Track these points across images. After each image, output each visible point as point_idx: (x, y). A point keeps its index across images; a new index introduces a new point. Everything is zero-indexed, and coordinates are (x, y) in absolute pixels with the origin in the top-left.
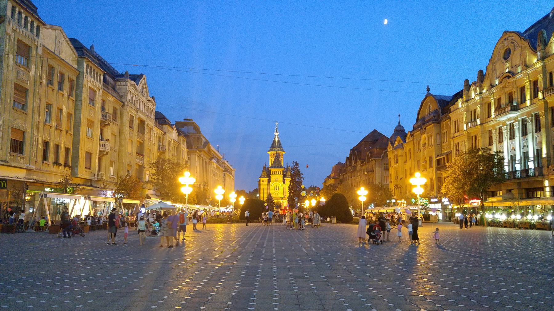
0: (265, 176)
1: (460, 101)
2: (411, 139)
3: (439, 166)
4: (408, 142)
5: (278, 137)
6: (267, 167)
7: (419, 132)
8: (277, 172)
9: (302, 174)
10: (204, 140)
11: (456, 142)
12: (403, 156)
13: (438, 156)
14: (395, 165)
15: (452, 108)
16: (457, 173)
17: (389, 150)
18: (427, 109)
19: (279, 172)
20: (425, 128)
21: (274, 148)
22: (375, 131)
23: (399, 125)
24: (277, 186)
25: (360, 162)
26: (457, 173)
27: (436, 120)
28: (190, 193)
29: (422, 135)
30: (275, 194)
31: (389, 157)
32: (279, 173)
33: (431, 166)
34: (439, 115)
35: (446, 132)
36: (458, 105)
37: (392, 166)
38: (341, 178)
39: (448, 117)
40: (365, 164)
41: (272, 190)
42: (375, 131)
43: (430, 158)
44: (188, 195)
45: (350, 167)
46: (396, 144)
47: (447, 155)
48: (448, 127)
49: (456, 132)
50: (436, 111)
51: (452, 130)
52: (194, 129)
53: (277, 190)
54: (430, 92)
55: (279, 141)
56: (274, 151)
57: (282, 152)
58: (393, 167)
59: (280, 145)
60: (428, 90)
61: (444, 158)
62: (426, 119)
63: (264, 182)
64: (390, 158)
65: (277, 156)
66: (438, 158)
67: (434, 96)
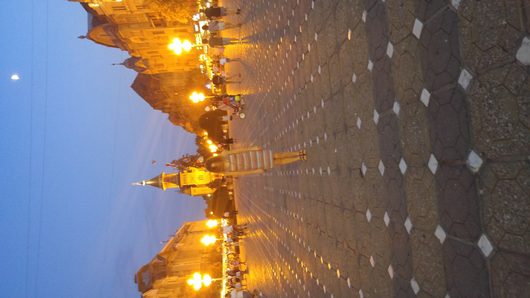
0: (189, 190)
1: (91, 5)
2: (137, 52)
3: (162, 25)
4: (140, 54)
5: (148, 181)
6: (180, 190)
7: (129, 45)
8: (184, 179)
9: (183, 156)
10: (156, 260)
11: (135, 9)
12: (155, 60)
13: (152, 26)
14: (165, 66)
15: (100, 13)
16: (166, 8)
17: (150, 73)
18: (104, 38)
20: (124, 39)
21: (160, 184)
22: (133, 86)
23: (124, 64)
24: (198, 178)
25: (166, 100)
26: (166, 8)
27: (114, 28)
28: (210, 277)
29: (131, 42)
30: (206, 178)
31: (158, 73)
32: (185, 177)
33: (163, 32)
34: (109, 26)
35: (126, 18)
36: (96, 7)
37: (167, 69)
38: (184, 117)
39: (110, 17)
40: (167, 94)
42: (133, 86)
43: (154, 33)
44: (212, 278)
45: (172, 109)
46: (143, 66)
47: (150, 17)
48: (120, 17)
49: (126, 9)
50: (105, 29)
51: (123, 13)
52: (145, 272)
53: (202, 178)
54: (85, 35)
55: (151, 180)
56: (162, 184)
57: (163, 176)
58: (167, 68)
59: (156, 179)
60: (82, 37)
61: (153, 20)
62: (114, 38)
64: (159, 71)
65: (168, 180)
66: (154, 26)
67: (90, 31)
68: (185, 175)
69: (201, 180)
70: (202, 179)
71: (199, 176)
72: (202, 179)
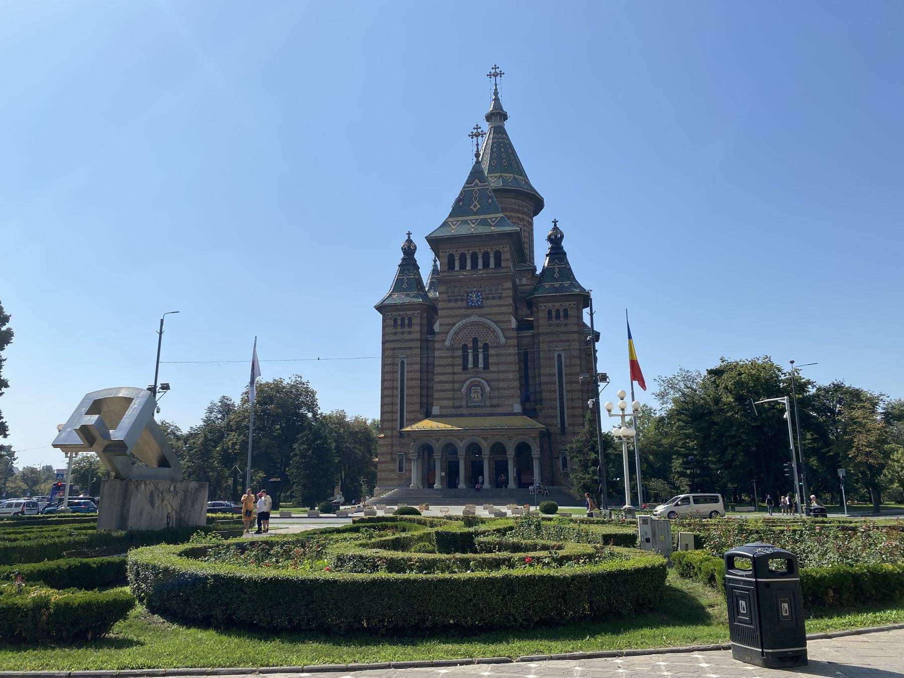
19: (486, 256)
24: (475, 340)
30: (469, 390)
32: (486, 265)
41: (449, 361)
63: (406, 329)
68: (498, 264)
69: (459, 361)
70: (465, 368)
71: (486, 347)
72: (465, 368)
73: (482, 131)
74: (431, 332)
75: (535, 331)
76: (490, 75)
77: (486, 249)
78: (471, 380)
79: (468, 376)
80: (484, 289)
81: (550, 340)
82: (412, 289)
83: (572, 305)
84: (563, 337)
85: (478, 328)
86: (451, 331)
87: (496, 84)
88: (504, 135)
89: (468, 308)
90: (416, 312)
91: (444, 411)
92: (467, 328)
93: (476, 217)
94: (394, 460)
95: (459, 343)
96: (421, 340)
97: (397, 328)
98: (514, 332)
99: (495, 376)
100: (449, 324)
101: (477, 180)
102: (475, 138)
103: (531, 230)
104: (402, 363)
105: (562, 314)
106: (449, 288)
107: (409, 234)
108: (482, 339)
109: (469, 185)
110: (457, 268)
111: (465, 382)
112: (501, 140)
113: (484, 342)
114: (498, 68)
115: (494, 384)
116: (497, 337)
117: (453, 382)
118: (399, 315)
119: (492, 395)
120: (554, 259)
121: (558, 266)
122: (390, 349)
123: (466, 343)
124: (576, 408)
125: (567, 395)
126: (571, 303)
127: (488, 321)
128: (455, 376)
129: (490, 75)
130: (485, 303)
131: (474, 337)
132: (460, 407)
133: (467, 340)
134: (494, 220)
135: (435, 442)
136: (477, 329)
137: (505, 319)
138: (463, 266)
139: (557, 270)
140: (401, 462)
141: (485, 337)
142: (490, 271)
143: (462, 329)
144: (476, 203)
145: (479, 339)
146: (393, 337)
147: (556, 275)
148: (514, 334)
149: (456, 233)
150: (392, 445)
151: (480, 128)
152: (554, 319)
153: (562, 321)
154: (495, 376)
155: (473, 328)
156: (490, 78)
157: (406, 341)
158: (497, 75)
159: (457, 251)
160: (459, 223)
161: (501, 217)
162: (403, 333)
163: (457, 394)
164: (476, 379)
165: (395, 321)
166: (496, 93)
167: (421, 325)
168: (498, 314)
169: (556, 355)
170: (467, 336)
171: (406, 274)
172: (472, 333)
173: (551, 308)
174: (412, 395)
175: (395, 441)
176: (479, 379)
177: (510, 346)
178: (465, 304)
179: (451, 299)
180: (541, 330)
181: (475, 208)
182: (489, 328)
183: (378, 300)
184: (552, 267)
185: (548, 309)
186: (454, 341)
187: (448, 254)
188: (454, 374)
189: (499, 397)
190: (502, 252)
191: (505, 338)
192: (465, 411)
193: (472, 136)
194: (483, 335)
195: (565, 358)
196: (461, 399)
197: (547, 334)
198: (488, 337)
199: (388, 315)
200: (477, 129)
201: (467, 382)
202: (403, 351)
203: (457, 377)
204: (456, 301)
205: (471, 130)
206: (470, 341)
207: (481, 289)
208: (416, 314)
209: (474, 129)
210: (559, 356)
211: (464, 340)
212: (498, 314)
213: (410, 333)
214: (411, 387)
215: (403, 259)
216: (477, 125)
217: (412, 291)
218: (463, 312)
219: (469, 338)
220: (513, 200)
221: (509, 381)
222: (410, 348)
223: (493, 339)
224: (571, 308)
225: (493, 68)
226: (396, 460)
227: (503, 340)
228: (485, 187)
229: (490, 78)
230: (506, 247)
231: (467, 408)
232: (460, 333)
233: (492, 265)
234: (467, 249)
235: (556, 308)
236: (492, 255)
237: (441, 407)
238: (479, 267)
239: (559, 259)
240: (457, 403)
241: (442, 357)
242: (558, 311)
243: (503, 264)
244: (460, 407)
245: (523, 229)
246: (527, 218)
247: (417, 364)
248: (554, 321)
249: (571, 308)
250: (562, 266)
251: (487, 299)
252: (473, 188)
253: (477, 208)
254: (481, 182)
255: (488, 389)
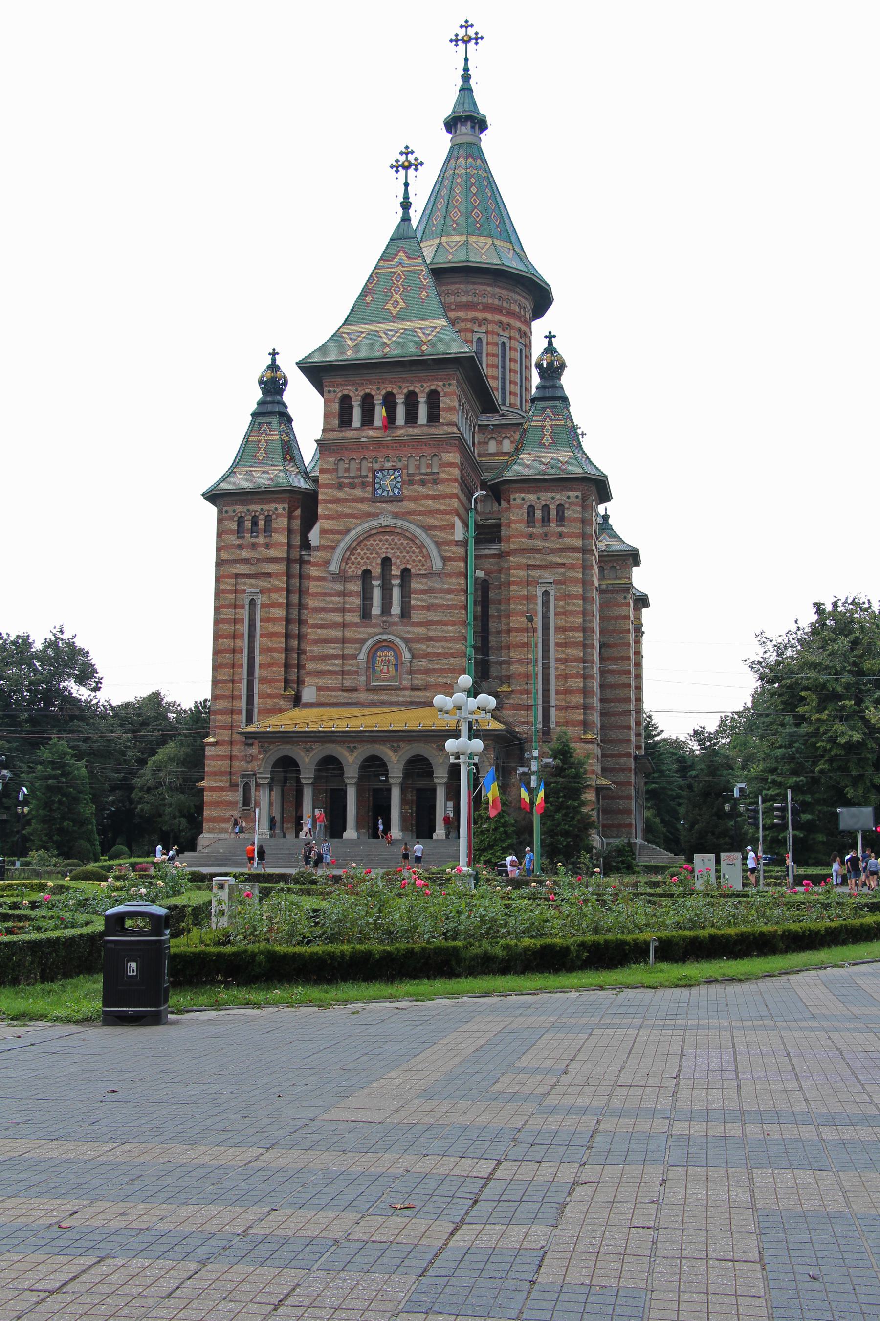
8: (389, 402)
19: (411, 400)
24: (386, 562)
32: (411, 417)
41: (336, 602)
53: (386, 608)
63: (261, 539)
68: (434, 417)
69: (356, 602)
70: (366, 614)
72: (366, 614)
73: (416, 159)
74: (306, 545)
75: (503, 546)
76: (455, 40)
77: (411, 388)
78: (375, 638)
79: (371, 630)
80: (406, 463)
81: (530, 563)
82: (274, 461)
83: (573, 499)
84: (555, 559)
85: (393, 540)
86: (342, 545)
87: (466, 60)
88: (479, 162)
89: (375, 500)
90: (280, 507)
91: (325, 696)
92: (372, 539)
93: (395, 326)
94: (234, 786)
95: (356, 567)
96: (289, 561)
97: (244, 537)
98: (458, 548)
99: (421, 631)
100: (339, 532)
101: (401, 254)
102: (402, 172)
103: (525, 346)
104: (252, 603)
105: (553, 514)
106: (339, 461)
107: (274, 354)
108: (398, 560)
109: (386, 263)
110: (356, 422)
111: (364, 641)
112: (472, 171)
113: (403, 567)
114: (472, 26)
115: (420, 647)
116: (428, 557)
117: (344, 641)
118: (248, 510)
119: (415, 666)
120: (545, 408)
121: (550, 423)
122: (229, 577)
123: (369, 568)
124: (571, 692)
125: (557, 668)
126: (570, 494)
127: (412, 527)
128: (346, 630)
129: (457, 41)
130: (408, 491)
131: (383, 556)
132: (354, 690)
133: (371, 563)
134: (428, 331)
135: (302, 754)
136: (390, 541)
137: (444, 523)
138: (368, 419)
139: (548, 430)
140: (247, 788)
141: (404, 557)
142: (417, 431)
143: (362, 541)
144: (397, 297)
145: (393, 560)
146: (235, 554)
147: (547, 440)
148: (459, 551)
149: (354, 356)
150: (231, 758)
151: (412, 152)
152: (538, 525)
153: (553, 528)
154: (421, 631)
155: (384, 539)
156: (456, 45)
157: (260, 561)
158: (469, 41)
159: (357, 390)
160: (363, 336)
161: (442, 327)
162: (254, 546)
163: (350, 665)
164: (385, 636)
165: (240, 521)
166: (466, 77)
167: (290, 531)
168: (430, 513)
169: (540, 593)
170: (371, 554)
171: (264, 432)
172: (381, 549)
173: (533, 503)
174: (270, 666)
175: (238, 750)
176: (390, 637)
177: (450, 575)
178: (368, 492)
179: (343, 483)
180: (514, 544)
181: (395, 308)
182: (413, 539)
183: (208, 483)
184: (540, 423)
185: (529, 504)
186: (347, 563)
187: (340, 395)
188: (344, 626)
189: (427, 672)
190: (442, 394)
191: (445, 559)
192: (362, 696)
193: (396, 167)
194: (401, 552)
195: (557, 598)
196: (356, 673)
197: (523, 552)
198: (411, 557)
199: (227, 512)
200: (407, 154)
201: (370, 643)
202: (253, 581)
203: (350, 633)
204: (352, 486)
205: (394, 155)
206: (377, 564)
207: (399, 465)
208: (280, 510)
209: (401, 153)
210: (546, 593)
211: (365, 562)
212: (430, 513)
213: (267, 546)
214: (269, 650)
215: (261, 403)
216: (407, 147)
217: (272, 465)
218: (364, 507)
219: (374, 558)
220: (489, 289)
221: (447, 640)
222: (268, 575)
223: (420, 561)
224: (571, 504)
225: (461, 27)
226: (237, 785)
227: (438, 563)
228: (417, 268)
229: (456, 45)
230: (450, 385)
231: (368, 690)
232: (359, 548)
233: (422, 418)
234: (375, 387)
235: (543, 503)
236: (422, 399)
237: (320, 689)
238: (420, 421)
239: (552, 408)
240: (349, 681)
241: (324, 594)
242: (546, 508)
243: (443, 417)
244: (354, 690)
245: (507, 345)
246: (518, 324)
247: (279, 605)
248: (539, 529)
249: (571, 504)
250: (558, 423)
251: (411, 483)
252: (393, 270)
253: (398, 309)
254: (409, 258)
255: (407, 656)
